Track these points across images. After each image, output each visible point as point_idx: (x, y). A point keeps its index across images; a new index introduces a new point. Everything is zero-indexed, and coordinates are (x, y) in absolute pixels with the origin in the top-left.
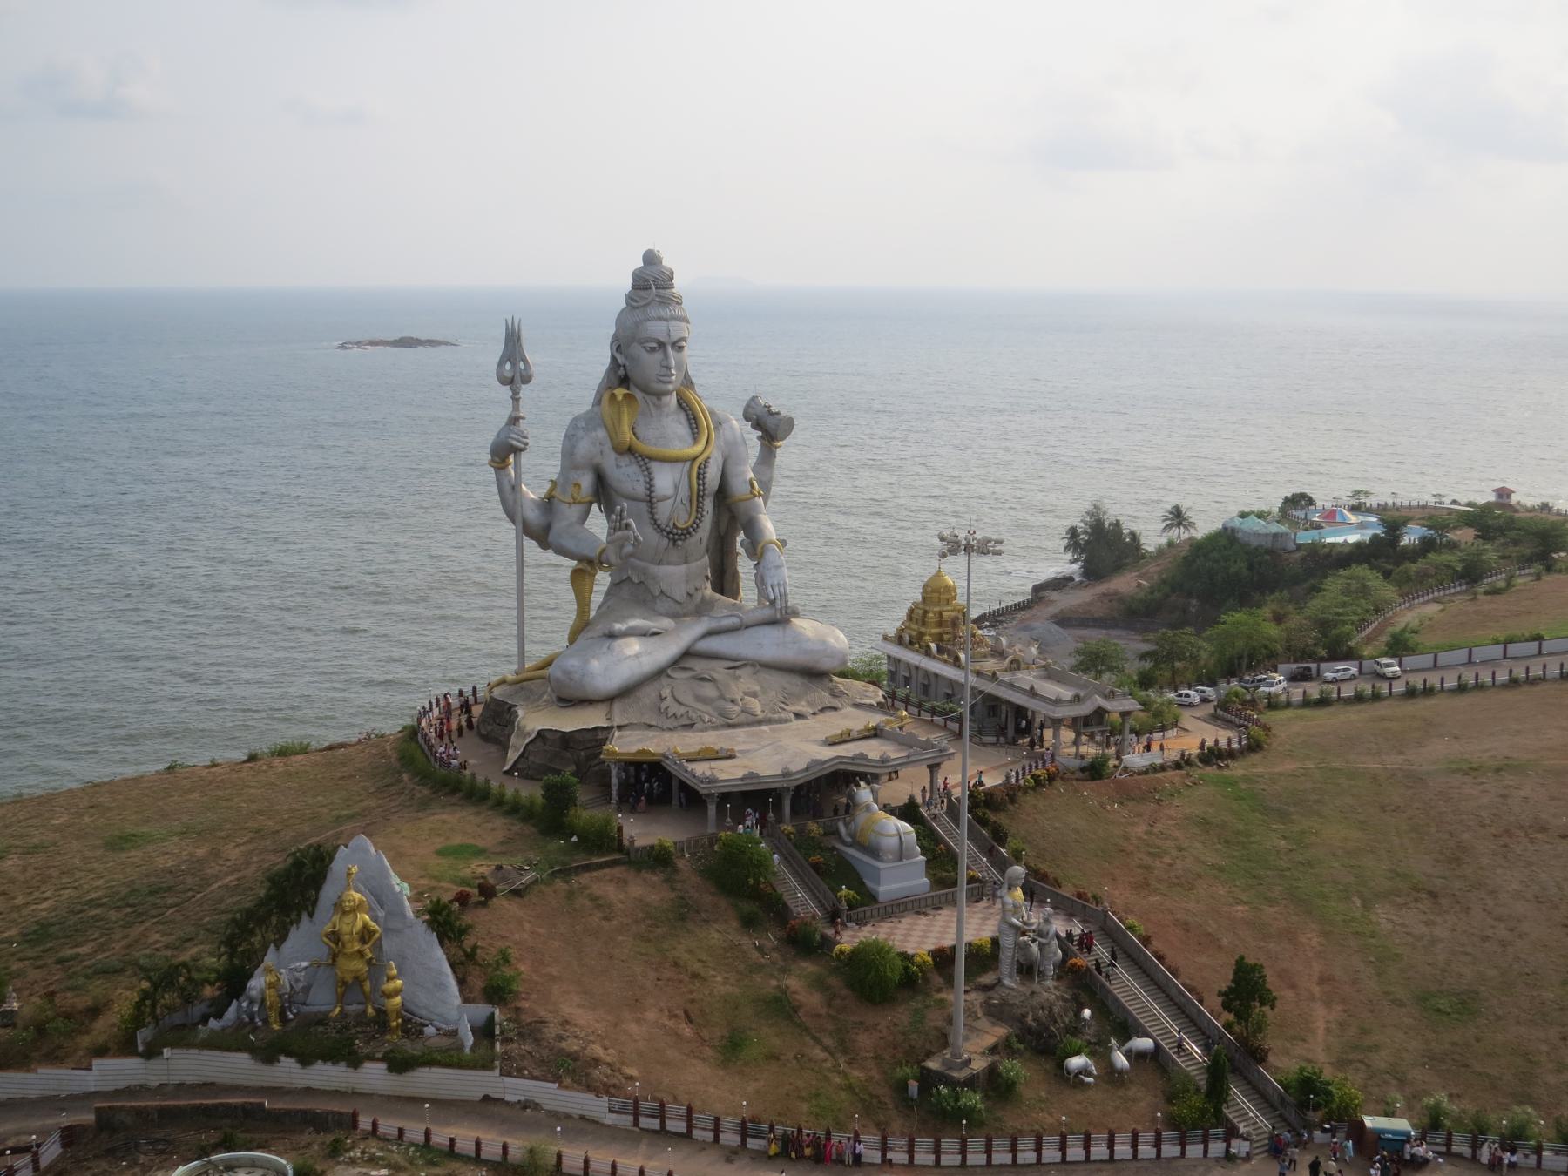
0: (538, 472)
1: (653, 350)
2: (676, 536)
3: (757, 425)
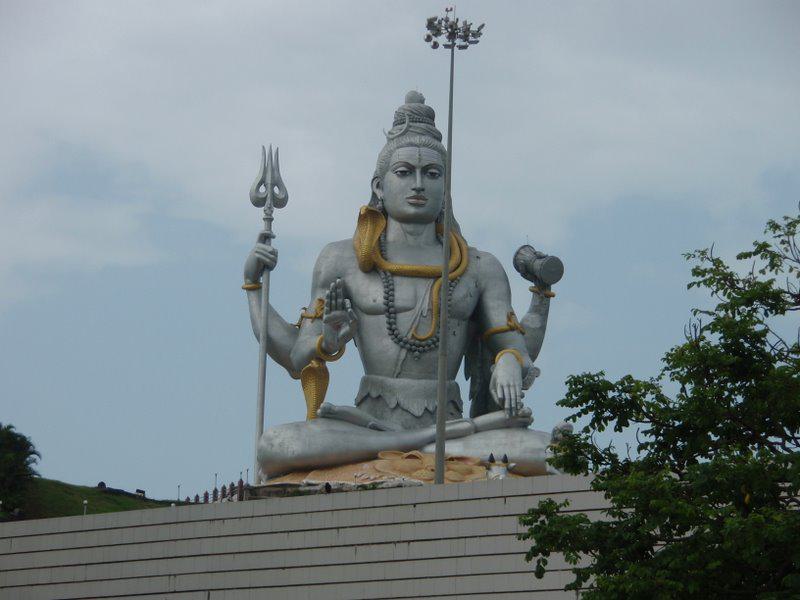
0: (293, 294)
1: (403, 174)
2: (416, 349)
3: (526, 271)
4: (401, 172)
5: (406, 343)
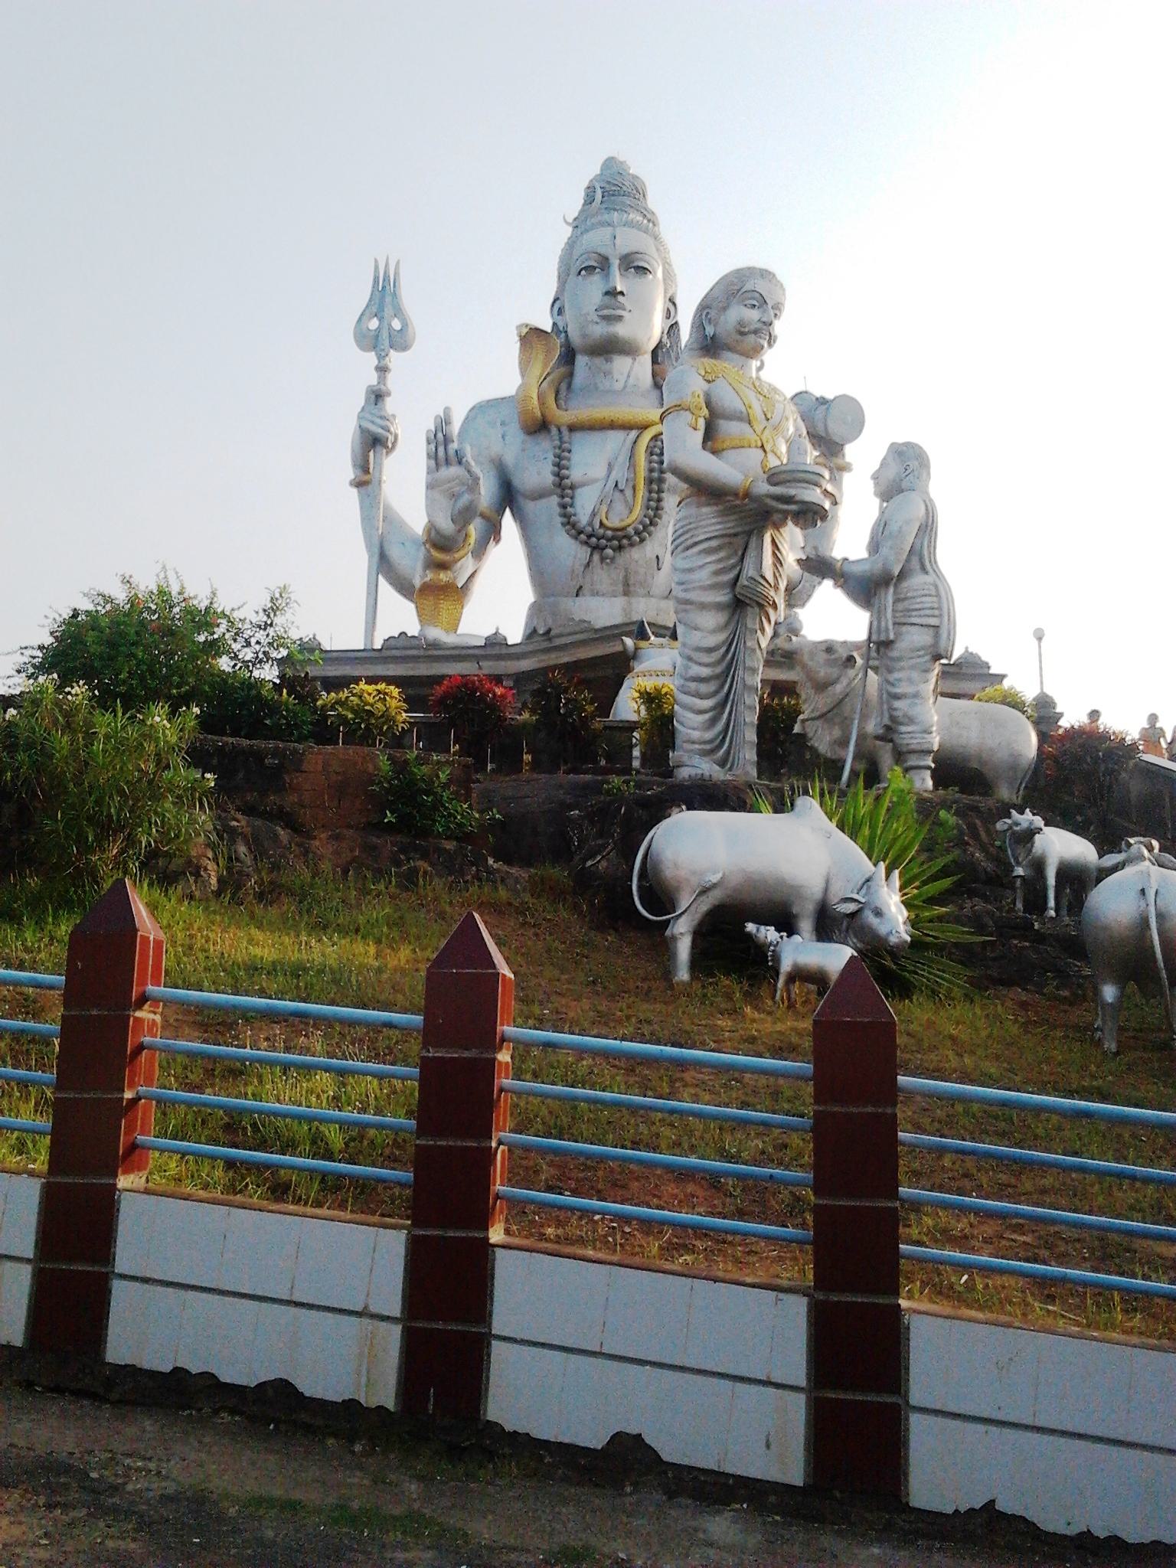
1: (590, 269)
4: (585, 268)
5: (589, 536)
